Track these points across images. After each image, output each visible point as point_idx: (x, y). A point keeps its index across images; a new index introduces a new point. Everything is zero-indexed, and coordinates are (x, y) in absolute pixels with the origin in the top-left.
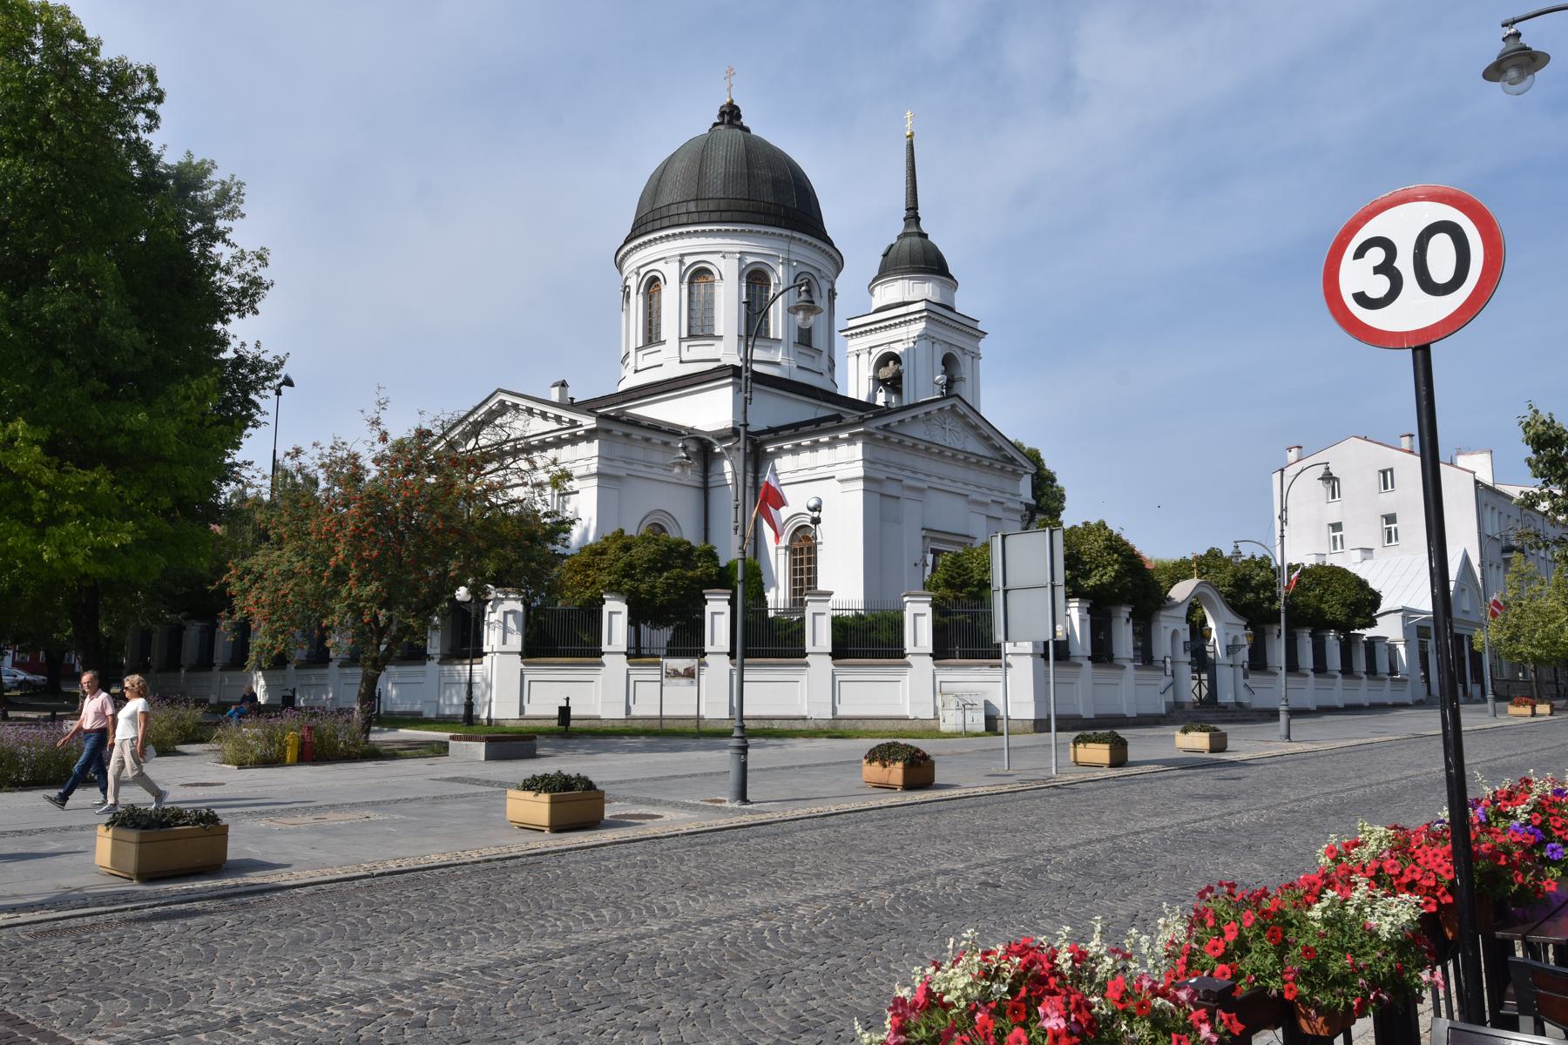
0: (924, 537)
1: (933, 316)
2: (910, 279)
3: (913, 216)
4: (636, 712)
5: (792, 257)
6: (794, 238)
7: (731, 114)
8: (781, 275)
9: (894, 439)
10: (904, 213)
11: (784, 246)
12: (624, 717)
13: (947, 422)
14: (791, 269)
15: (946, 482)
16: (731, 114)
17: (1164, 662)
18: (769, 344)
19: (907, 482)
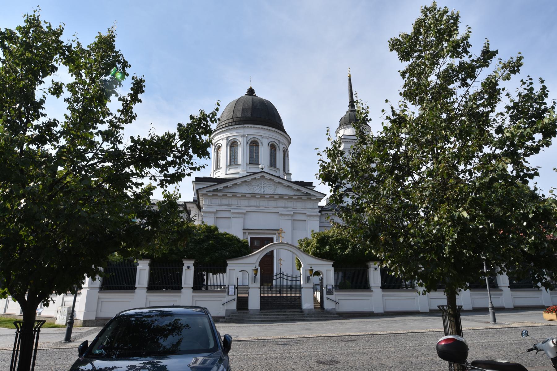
0: (244, 233)
1: (346, 140)
2: (343, 128)
3: (352, 103)
4: (8, 312)
5: (245, 134)
6: (245, 127)
7: (251, 92)
8: (241, 141)
9: (220, 194)
10: (348, 104)
11: (242, 130)
12: (3, 313)
13: (262, 183)
14: (245, 138)
15: (270, 208)
16: (251, 92)
17: (228, 288)
18: (236, 167)
19: (232, 211)
